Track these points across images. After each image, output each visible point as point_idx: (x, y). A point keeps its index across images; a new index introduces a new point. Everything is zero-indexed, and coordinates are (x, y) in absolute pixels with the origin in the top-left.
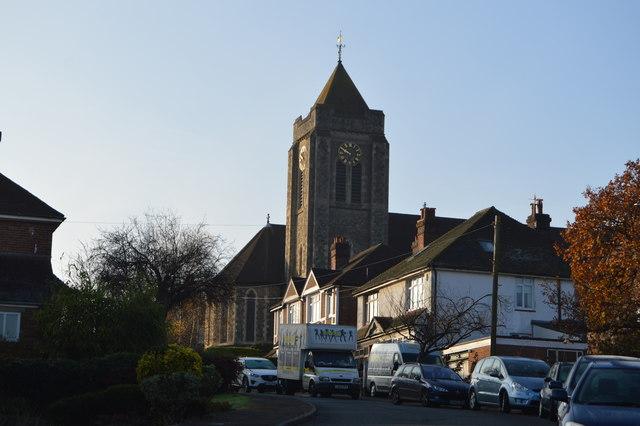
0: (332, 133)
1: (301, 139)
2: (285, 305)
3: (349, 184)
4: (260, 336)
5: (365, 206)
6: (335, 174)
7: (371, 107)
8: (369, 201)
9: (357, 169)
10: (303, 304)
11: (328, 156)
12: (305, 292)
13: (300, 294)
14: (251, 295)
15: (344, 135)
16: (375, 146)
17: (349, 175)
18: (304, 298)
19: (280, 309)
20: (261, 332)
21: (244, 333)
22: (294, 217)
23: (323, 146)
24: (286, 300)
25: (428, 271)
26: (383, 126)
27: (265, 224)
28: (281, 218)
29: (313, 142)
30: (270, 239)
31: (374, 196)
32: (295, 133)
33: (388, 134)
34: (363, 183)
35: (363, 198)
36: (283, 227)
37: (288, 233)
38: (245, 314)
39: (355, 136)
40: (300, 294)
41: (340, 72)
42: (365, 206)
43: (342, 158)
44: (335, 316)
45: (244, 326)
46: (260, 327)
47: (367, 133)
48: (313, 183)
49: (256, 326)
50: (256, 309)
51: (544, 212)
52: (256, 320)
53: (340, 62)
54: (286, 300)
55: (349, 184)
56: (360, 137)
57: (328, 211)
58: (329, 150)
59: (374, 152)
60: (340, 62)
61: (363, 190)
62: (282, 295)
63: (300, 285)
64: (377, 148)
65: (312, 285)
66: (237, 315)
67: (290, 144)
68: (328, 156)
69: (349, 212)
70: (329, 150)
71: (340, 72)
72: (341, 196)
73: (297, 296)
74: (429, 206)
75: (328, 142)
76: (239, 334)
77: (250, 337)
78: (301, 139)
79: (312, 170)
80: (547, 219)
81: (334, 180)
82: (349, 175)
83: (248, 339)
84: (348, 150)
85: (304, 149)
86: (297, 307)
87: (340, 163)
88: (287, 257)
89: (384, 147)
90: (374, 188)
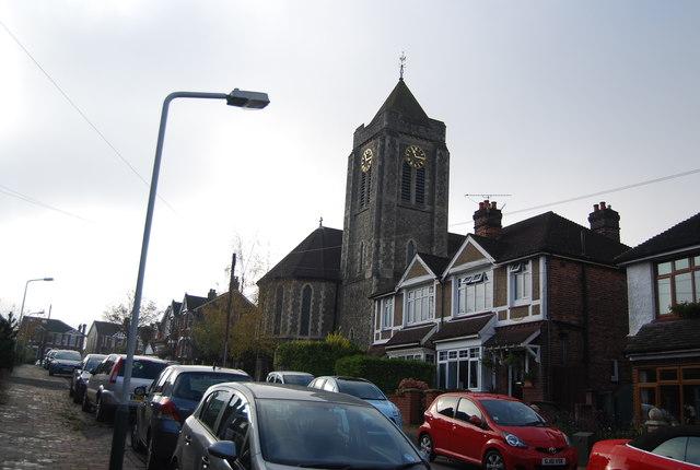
3: (414, 185)
4: (315, 331)
7: (432, 114)
8: (432, 203)
9: (421, 172)
10: (444, 285)
12: (450, 270)
17: (414, 176)
18: (449, 276)
19: (391, 297)
23: (393, 144)
24: (403, 284)
27: (317, 226)
28: (336, 221)
29: (383, 140)
30: (322, 242)
34: (427, 187)
35: (426, 201)
41: (401, 84)
42: (428, 208)
46: (315, 321)
47: (431, 141)
48: (382, 179)
49: (311, 320)
50: (312, 304)
53: (401, 79)
55: (414, 185)
58: (398, 149)
60: (401, 79)
61: (427, 193)
62: (398, 276)
66: (293, 310)
67: (349, 148)
70: (398, 149)
71: (401, 84)
72: (406, 195)
73: (432, 276)
76: (294, 328)
78: (365, 143)
79: (381, 168)
82: (414, 176)
83: (301, 334)
84: (416, 152)
86: (429, 294)
87: (406, 164)
88: (344, 257)
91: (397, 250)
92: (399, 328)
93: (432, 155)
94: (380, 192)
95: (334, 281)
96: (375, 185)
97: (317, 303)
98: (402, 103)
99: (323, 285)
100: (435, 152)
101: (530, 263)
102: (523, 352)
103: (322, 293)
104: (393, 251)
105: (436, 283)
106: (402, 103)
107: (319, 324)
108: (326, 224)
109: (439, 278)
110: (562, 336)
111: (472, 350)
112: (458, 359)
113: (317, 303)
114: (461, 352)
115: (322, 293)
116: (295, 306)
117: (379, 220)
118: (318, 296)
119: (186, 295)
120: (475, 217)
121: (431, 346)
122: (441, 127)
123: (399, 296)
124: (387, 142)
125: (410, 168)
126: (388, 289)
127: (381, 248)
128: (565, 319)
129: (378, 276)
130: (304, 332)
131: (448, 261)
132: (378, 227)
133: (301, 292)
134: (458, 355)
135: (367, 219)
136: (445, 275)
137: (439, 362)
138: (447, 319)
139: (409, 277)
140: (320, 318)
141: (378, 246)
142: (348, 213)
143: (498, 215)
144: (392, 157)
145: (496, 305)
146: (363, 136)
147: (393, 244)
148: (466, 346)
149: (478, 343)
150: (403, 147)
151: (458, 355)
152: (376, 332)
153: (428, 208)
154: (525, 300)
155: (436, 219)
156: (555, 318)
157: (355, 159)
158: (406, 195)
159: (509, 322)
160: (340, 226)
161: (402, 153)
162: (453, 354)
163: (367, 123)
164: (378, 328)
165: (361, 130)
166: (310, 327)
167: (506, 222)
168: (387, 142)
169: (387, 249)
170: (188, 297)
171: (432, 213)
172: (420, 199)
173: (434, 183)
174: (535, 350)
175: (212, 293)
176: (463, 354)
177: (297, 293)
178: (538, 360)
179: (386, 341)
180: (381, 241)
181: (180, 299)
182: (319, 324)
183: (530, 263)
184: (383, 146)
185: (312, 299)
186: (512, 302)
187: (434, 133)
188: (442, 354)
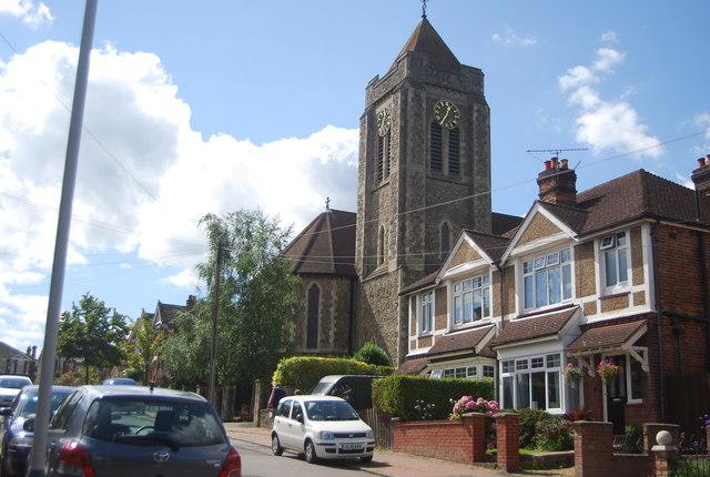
3: (446, 151)
4: (325, 342)
7: (462, 62)
8: (470, 173)
10: (504, 273)
11: (424, 113)
12: (513, 250)
13: (495, 255)
14: (314, 292)
16: (476, 108)
20: (328, 337)
21: (305, 336)
22: (371, 195)
23: (417, 98)
24: (447, 273)
26: (482, 87)
28: (348, 202)
29: (405, 94)
30: (334, 228)
31: (476, 168)
32: (369, 96)
34: (462, 152)
35: (462, 170)
36: (351, 217)
42: (464, 180)
44: (646, 287)
45: (305, 328)
46: (326, 331)
49: (320, 328)
50: (320, 308)
52: (320, 322)
53: (424, 16)
55: (446, 151)
56: (457, 96)
57: (423, 182)
58: (424, 106)
59: (475, 115)
60: (424, 16)
61: (462, 161)
64: (478, 111)
68: (424, 113)
70: (424, 106)
73: (486, 260)
75: (424, 96)
79: (404, 129)
84: (447, 110)
85: (391, 106)
87: (436, 127)
90: (476, 158)
91: (428, 234)
92: (443, 332)
93: (468, 111)
94: (403, 160)
95: (347, 277)
96: (395, 152)
97: (326, 307)
99: (334, 282)
100: (471, 108)
101: (628, 235)
103: (333, 293)
104: (423, 235)
105: (494, 268)
107: (331, 333)
108: (334, 206)
109: (497, 263)
110: (676, 333)
111: (550, 358)
112: (530, 370)
113: (326, 307)
114: (534, 361)
118: (328, 296)
119: (159, 303)
120: (540, 182)
122: (477, 75)
123: (441, 291)
124: (410, 95)
125: (440, 128)
126: (422, 276)
127: (407, 234)
128: (679, 311)
129: (405, 269)
131: (508, 241)
133: (307, 293)
134: (529, 364)
135: (389, 196)
136: (504, 258)
137: (502, 375)
138: (512, 317)
139: (455, 263)
140: (332, 326)
141: (402, 229)
142: (363, 190)
143: (571, 176)
144: (418, 115)
145: (579, 295)
146: (379, 90)
147: (423, 226)
148: (541, 351)
149: (558, 348)
150: (431, 102)
151: (529, 364)
152: (411, 338)
153: (464, 180)
154: (629, 287)
156: (666, 309)
158: (436, 164)
160: (355, 211)
161: (430, 111)
162: (523, 364)
164: (414, 333)
165: (375, 83)
167: (582, 186)
168: (410, 95)
169: (416, 230)
170: (162, 307)
172: (454, 168)
173: (470, 148)
174: (641, 354)
175: (191, 300)
176: (537, 362)
178: (645, 368)
179: (426, 350)
180: (407, 224)
181: (152, 309)
182: (331, 333)
183: (628, 235)
184: (404, 102)
185: (321, 300)
186: (603, 290)
188: (505, 364)
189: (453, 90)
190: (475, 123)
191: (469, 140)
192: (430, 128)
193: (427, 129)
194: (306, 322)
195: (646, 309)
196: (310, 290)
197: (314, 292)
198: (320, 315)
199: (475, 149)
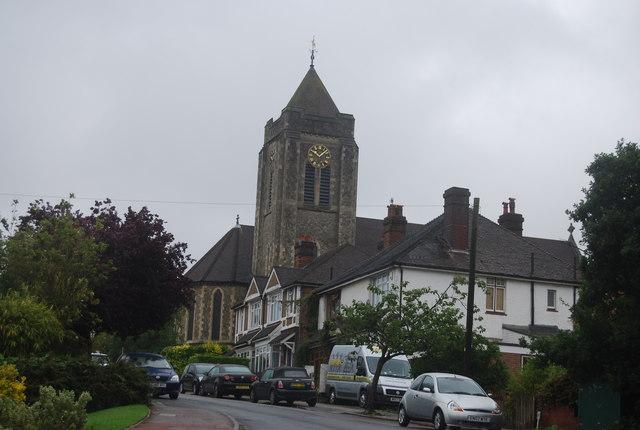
0: (302, 135)
1: (272, 140)
2: (247, 303)
3: (318, 186)
4: (225, 335)
5: (333, 208)
6: (304, 176)
7: (342, 110)
8: (338, 204)
9: (326, 171)
11: (298, 158)
12: (266, 291)
13: (262, 291)
14: (218, 296)
15: (311, 140)
17: (318, 177)
21: (210, 331)
22: (261, 217)
23: (293, 147)
24: (248, 299)
25: (395, 268)
26: (353, 130)
27: (232, 225)
28: (249, 219)
30: (237, 241)
33: (359, 136)
35: (331, 201)
37: (256, 234)
38: (211, 313)
39: (325, 139)
40: (262, 291)
41: (312, 73)
42: (333, 208)
43: (312, 160)
50: (222, 308)
51: (516, 212)
53: (312, 66)
54: (248, 299)
55: (318, 186)
57: (295, 213)
58: (299, 151)
59: (344, 155)
60: (312, 66)
61: (332, 193)
63: (262, 281)
65: (273, 283)
66: (204, 314)
67: (261, 146)
69: (317, 214)
70: (299, 151)
71: (312, 73)
72: (309, 197)
74: (395, 203)
75: (298, 144)
76: (205, 333)
77: (215, 337)
78: (272, 140)
80: (519, 219)
81: (303, 182)
82: (318, 177)
84: (319, 152)
87: (310, 168)
88: (255, 261)
89: (352, 151)
90: (342, 191)
92: (246, 332)
93: (336, 152)
98: (312, 91)
99: (233, 289)
100: (341, 150)
102: (284, 346)
103: (232, 297)
106: (312, 91)
115: (232, 297)
116: (206, 311)
117: (278, 224)
118: (228, 298)
121: (253, 345)
122: (349, 121)
123: (247, 308)
130: (215, 337)
132: (278, 231)
133: (212, 297)
135: (270, 222)
138: (265, 326)
144: (293, 160)
150: (305, 148)
155: (341, 220)
157: (264, 155)
159: (286, 327)
160: (252, 223)
161: (306, 156)
163: (276, 116)
166: (221, 332)
168: (287, 144)
169: (287, 253)
171: (337, 213)
172: (325, 199)
177: (207, 297)
185: (223, 303)
187: (344, 125)
189: (326, 135)
190: (343, 162)
191: (338, 176)
192: (304, 169)
193: (301, 169)
194: (211, 319)
195: (293, 325)
196: (216, 295)
197: (218, 296)
198: (222, 314)
199: (343, 184)
